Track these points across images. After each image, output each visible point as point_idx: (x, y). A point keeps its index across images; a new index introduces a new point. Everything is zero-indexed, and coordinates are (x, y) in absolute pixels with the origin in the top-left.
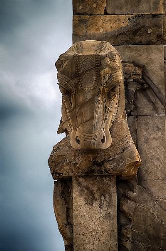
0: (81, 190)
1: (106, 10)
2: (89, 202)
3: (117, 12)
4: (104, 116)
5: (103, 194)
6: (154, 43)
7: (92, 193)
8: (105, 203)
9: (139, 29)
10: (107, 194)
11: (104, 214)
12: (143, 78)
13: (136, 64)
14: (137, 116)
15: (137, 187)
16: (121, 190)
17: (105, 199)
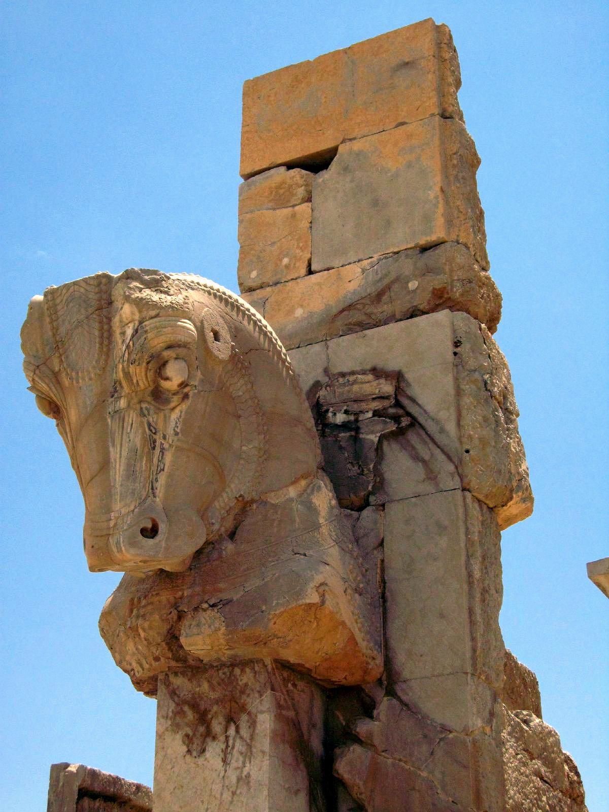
0: (178, 713)
1: (309, 265)
2: (195, 746)
3: (337, 263)
4: (150, 460)
5: (231, 719)
6: (424, 313)
7: (203, 718)
8: (239, 746)
9: (388, 287)
10: (244, 717)
11: (234, 779)
13: (377, 372)
14: (383, 505)
15: (384, 705)
16: (341, 718)
17: (237, 731)
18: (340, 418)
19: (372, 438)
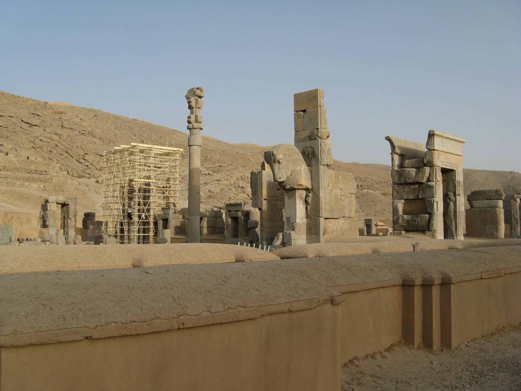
3: (306, 130)
5: (292, 196)
12: (313, 152)
13: (311, 147)
18: (307, 153)
19: (310, 157)
